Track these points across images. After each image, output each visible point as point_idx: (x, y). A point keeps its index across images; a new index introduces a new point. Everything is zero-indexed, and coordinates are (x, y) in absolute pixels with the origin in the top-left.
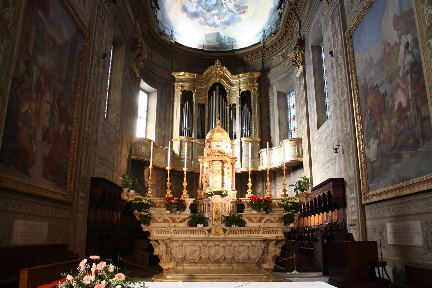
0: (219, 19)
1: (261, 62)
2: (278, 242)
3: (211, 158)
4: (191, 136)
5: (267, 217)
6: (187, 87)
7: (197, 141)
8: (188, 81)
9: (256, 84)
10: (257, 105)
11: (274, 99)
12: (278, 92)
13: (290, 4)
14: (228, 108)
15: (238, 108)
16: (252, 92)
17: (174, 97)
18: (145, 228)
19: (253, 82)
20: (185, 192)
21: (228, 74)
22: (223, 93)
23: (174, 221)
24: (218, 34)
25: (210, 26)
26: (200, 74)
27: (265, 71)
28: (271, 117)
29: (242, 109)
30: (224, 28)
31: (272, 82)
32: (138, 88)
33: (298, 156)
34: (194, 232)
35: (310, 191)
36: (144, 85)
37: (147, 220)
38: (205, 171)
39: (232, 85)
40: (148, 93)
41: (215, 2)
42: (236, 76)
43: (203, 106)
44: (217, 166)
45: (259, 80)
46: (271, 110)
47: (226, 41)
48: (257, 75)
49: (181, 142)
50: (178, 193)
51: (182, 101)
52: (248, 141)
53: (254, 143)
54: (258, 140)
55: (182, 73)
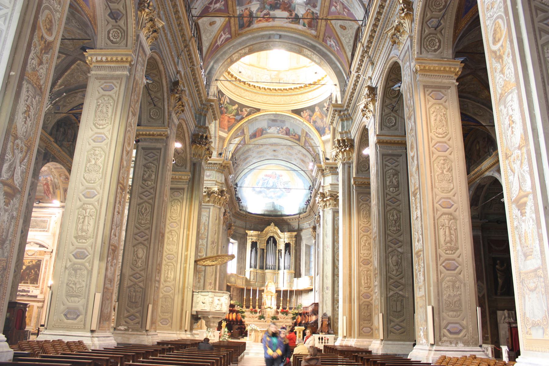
0: (274, 194)
1: (297, 224)
2: (290, 326)
3: (267, 294)
4: (256, 268)
5: (287, 317)
6: (254, 239)
7: (260, 271)
8: (255, 236)
9: (294, 239)
10: (294, 251)
11: (303, 248)
12: (306, 244)
13: (310, 207)
14: (277, 252)
15: (283, 252)
16: (291, 244)
17: (246, 245)
18: (243, 320)
19: (291, 238)
20: (257, 307)
21: (279, 231)
22: (275, 242)
23: (253, 317)
24: (273, 203)
25: (269, 198)
26: (262, 231)
27: (299, 230)
28: (301, 259)
29: (285, 253)
30: (277, 200)
31: (303, 238)
32: (228, 241)
33: (311, 285)
34: (260, 322)
35: (302, 308)
36: (232, 240)
37: (243, 317)
38: (265, 298)
39: (280, 238)
40: (232, 243)
41: (272, 185)
42: (283, 233)
43: (263, 250)
44: (270, 297)
45: (296, 236)
46: (302, 254)
47: (278, 208)
48: (295, 233)
49: (250, 272)
50: (254, 307)
51: (251, 248)
52: (288, 272)
53: (291, 273)
54: (293, 271)
55: (252, 231)
